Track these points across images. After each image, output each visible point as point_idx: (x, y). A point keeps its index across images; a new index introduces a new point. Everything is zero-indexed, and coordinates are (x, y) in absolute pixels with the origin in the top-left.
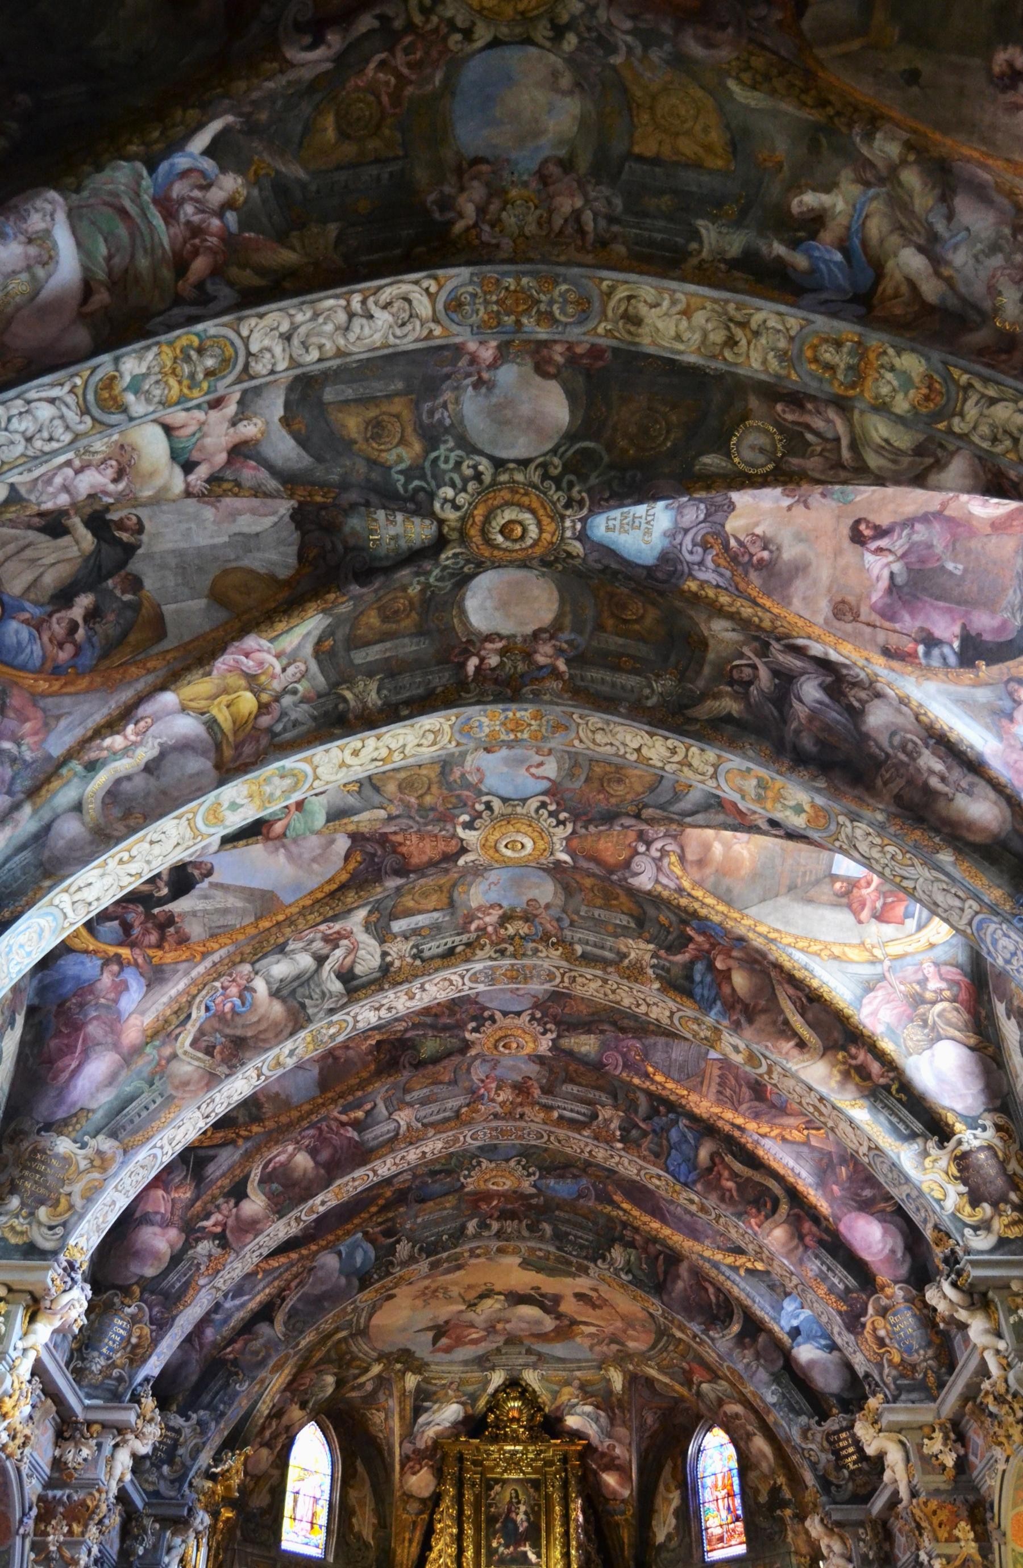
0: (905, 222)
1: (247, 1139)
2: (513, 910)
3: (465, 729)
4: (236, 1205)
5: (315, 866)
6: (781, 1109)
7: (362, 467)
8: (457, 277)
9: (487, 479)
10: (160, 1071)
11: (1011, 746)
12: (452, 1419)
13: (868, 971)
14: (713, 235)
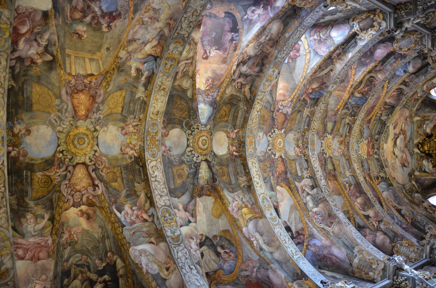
0: (139, 50)
1: (353, 214)
2: (295, 144)
3: (252, 155)
4: (371, 218)
5: (284, 195)
6: (347, 75)
7: (189, 180)
8: (147, 155)
9: (192, 149)
10: (337, 236)
11: (259, 20)
13: (312, 54)
14: (139, 94)
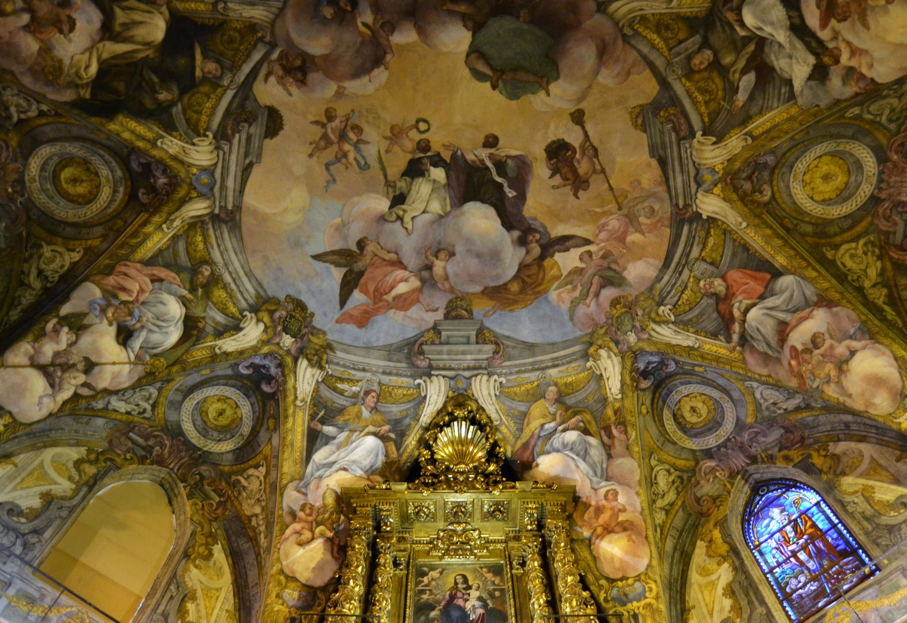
12: (367, 463)
